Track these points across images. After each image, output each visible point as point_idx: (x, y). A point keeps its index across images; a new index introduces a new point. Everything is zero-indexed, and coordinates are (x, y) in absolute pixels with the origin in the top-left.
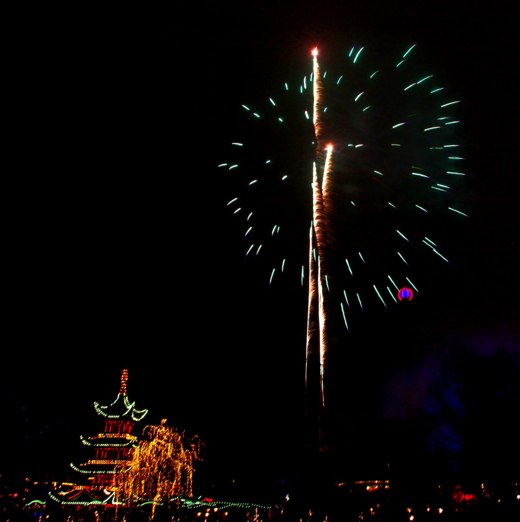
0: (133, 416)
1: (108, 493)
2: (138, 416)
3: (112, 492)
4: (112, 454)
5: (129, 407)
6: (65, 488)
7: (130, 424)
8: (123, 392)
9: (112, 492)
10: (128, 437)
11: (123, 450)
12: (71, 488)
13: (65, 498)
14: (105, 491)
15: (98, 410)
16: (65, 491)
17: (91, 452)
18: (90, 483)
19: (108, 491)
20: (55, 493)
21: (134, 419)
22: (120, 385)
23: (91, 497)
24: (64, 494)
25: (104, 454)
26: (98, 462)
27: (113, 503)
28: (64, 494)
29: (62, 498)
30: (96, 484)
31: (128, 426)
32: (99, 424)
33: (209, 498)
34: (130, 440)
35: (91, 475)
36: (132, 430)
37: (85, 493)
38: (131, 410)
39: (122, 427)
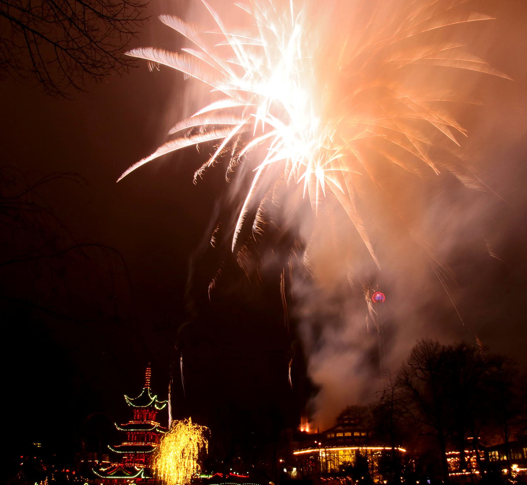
0: (156, 406)
1: (138, 469)
2: (160, 405)
3: (141, 468)
4: (140, 438)
5: (153, 399)
6: (105, 466)
7: (154, 412)
8: (148, 386)
9: (141, 468)
10: (152, 423)
11: (149, 434)
12: (109, 465)
13: (105, 474)
14: (135, 467)
15: (127, 401)
16: (104, 468)
17: (124, 437)
18: (124, 461)
19: (138, 468)
20: (97, 468)
21: (157, 408)
22: (144, 381)
23: (125, 473)
24: (103, 469)
25: (134, 437)
26: (130, 444)
27: (143, 477)
28: (103, 469)
29: (102, 473)
30: (129, 462)
31: (152, 414)
32: (129, 413)
33: (220, 473)
34: (154, 425)
35: (124, 455)
36: (156, 417)
37: (119, 469)
38: (154, 402)
39: (148, 415)
